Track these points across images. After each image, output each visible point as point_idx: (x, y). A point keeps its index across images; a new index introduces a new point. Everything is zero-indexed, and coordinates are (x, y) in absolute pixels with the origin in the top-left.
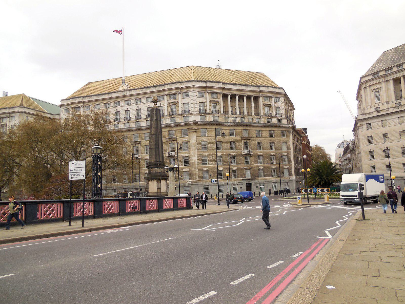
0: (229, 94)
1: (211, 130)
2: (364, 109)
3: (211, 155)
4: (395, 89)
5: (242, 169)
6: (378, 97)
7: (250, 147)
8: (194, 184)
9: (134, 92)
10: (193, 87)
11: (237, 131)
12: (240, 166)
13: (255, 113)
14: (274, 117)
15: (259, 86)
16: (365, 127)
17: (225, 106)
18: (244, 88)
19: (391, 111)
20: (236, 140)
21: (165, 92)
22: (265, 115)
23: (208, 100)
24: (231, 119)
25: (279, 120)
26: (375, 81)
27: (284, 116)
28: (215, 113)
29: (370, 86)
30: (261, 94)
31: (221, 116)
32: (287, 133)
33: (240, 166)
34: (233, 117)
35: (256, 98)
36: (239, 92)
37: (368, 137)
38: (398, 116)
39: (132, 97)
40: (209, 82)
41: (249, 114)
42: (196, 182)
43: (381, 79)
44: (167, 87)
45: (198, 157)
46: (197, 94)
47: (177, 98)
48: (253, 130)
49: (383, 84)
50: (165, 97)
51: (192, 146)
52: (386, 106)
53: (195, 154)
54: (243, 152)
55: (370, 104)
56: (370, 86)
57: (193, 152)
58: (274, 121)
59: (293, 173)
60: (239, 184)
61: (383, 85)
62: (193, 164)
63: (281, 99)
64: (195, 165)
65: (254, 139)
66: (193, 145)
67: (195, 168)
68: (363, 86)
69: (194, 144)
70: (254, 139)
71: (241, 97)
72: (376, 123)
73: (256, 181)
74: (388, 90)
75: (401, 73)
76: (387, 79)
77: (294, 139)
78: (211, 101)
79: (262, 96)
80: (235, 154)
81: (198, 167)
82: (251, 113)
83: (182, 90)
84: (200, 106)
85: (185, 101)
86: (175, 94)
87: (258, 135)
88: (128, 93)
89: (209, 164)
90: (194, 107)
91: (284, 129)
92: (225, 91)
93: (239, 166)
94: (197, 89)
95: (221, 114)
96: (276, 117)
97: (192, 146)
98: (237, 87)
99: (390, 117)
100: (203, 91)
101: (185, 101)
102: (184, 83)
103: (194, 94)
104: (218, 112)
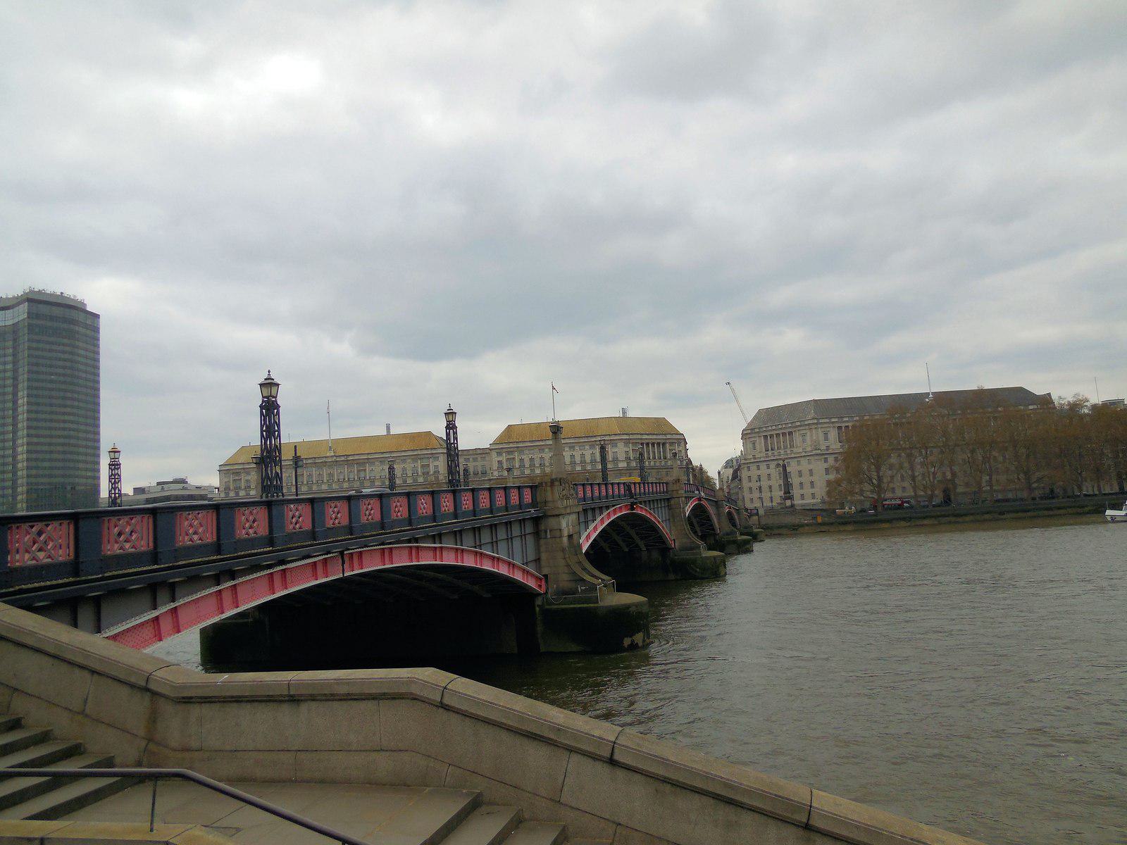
18: (655, 437)
35: (664, 444)
61: (757, 439)
71: (653, 444)
85: (615, 450)
90: (621, 456)
98: (650, 437)
100: (627, 442)
103: (621, 445)
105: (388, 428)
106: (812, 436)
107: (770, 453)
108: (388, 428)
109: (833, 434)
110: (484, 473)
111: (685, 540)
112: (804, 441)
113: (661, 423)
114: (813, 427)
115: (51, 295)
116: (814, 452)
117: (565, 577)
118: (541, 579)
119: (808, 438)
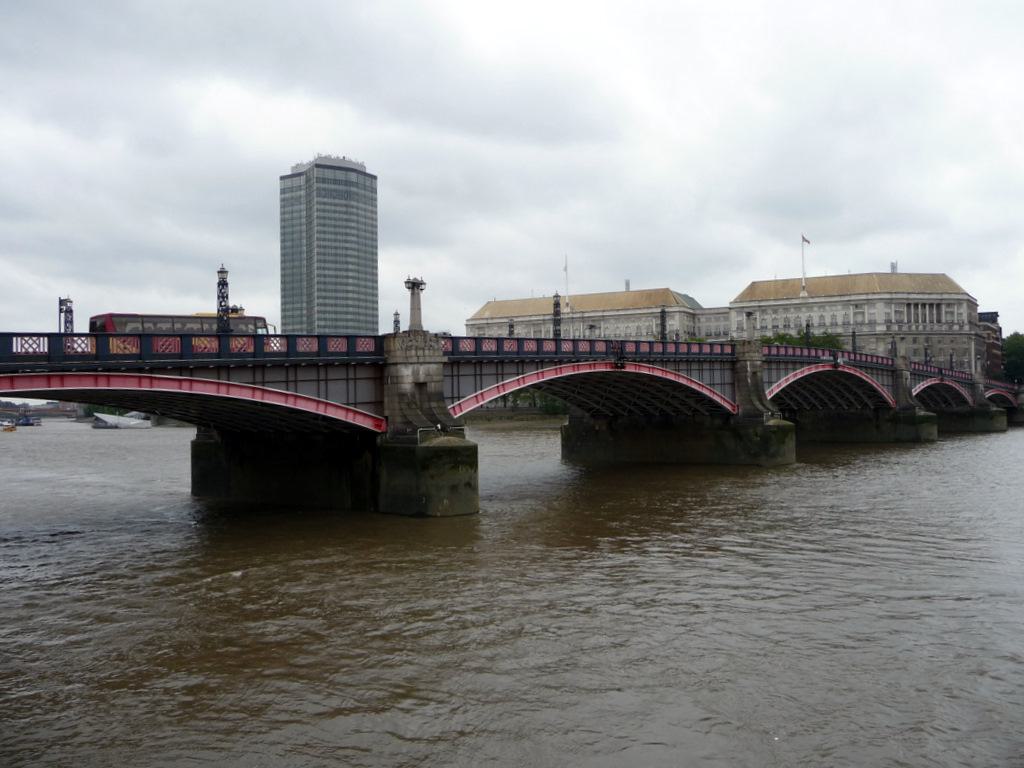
9: (817, 300)
15: (942, 294)
18: (926, 296)
22: (947, 323)
25: (961, 327)
27: (966, 322)
28: (899, 322)
30: (944, 302)
35: (939, 305)
44: (853, 298)
77: (976, 344)
78: (896, 311)
85: (872, 311)
87: (939, 342)
88: (811, 300)
90: (880, 318)
96: (958, 324)
100: (889, 302)
101: (872, 311)
104: (902, 322)
105: (627, 284)
108: (627, 284)
110: (726, 334)
111: (748, 407)
113: (942, 279)
115: (334, 160)
117: (399, 419)
118: (382, 420)
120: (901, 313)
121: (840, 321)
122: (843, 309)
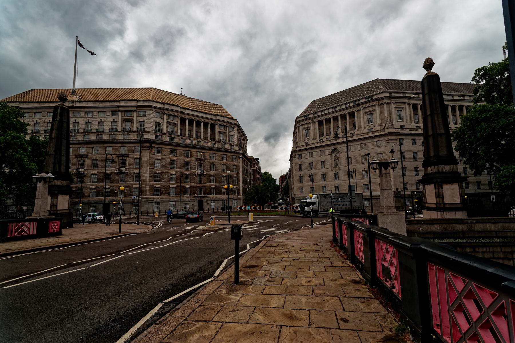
0: (187, 119)
1: (165, 149)
2: (297, 143)
3: (163, 173)
4: (319, 128)
5: (194, 187)
6: (307, 135)
7: (203, 168)
8: (143, 200)
9: (84, 104)
10: (150, 107)
11: (192, 152)
12: (193, 184)
13: (210, 138)
14: (228, 143)
15: (216, 115)
16: (297, 156)
17: (183, 129)
19: (316, 145)
20: (191, 160)
21: (120, 108)
22: (219, 141)
23: (165, 121)
24: (188, 141)
25: (232, 146)
26: (306, 121)
27: (236, 143)
29: (302, 125)
30: (217, 122)
31: (178, 137)
32: (238, 158)
33: (193, 184)
34: (190, 140)
35: (213, 127)
36: (197, 118)
37: (299, 164)
38: (321, 149)
39: (82, 109)
40: (168, 104)
41: (205, 138)
42: (146, 198)
43: (310, 120)
44: (122, 103)
45: (150, 174)
46: (154, 114)
47: (133, 115)
48: (208, 153)
49: (312, 124)
50: (120, 113)
51: (144, 163)
52: (312, 142)
53: (147, 170)
54: (197, 171)
55: (302, 139)
56: (302, 125)
57: (145, 169)
58: (227, 146)
59: (241, 192)
60: (191, 201)
62: (145, 181)
63: (234, 129)
64: (146, 181)
65: (208, 160)
66: (145, 162)
67: (146, 185)
68: (298, 125)
69: (146, 161)
70: (208, 160)
71: (198, 123)
72: (305, 154)
73: (208, 198)
74: (314, 129)
75: (324, 117)
76: (315, 120)
78: (168, 123)
79: (217, 124)
80: (189, 173)
81: (150, 184)
82: (207, 138)
83: (138, 109)
84: (156, 126)
86: (131, 111)
87: (212, 158)
88: (78, 105)
89: (161, 181)
90: (150, 126)
91: (235, 155)
92: (184, 115)
93: (192, 185)
94: (154, 109)
95: (178, 136)
96: (229, 143)
97: (144, 163)
99: (315, 150)
100: (160, 112)
102: (141, 102)
103: (151, 114)
104: (174, 133)
106: (382, 112)
107: (325, 139)
109: (407, 112)
112: (371, 120)
114: (385, 101)
116: (386, 131)
119: (377, 116)
120: (174, 125)
121: (107, 127)
122: (112, 116)
